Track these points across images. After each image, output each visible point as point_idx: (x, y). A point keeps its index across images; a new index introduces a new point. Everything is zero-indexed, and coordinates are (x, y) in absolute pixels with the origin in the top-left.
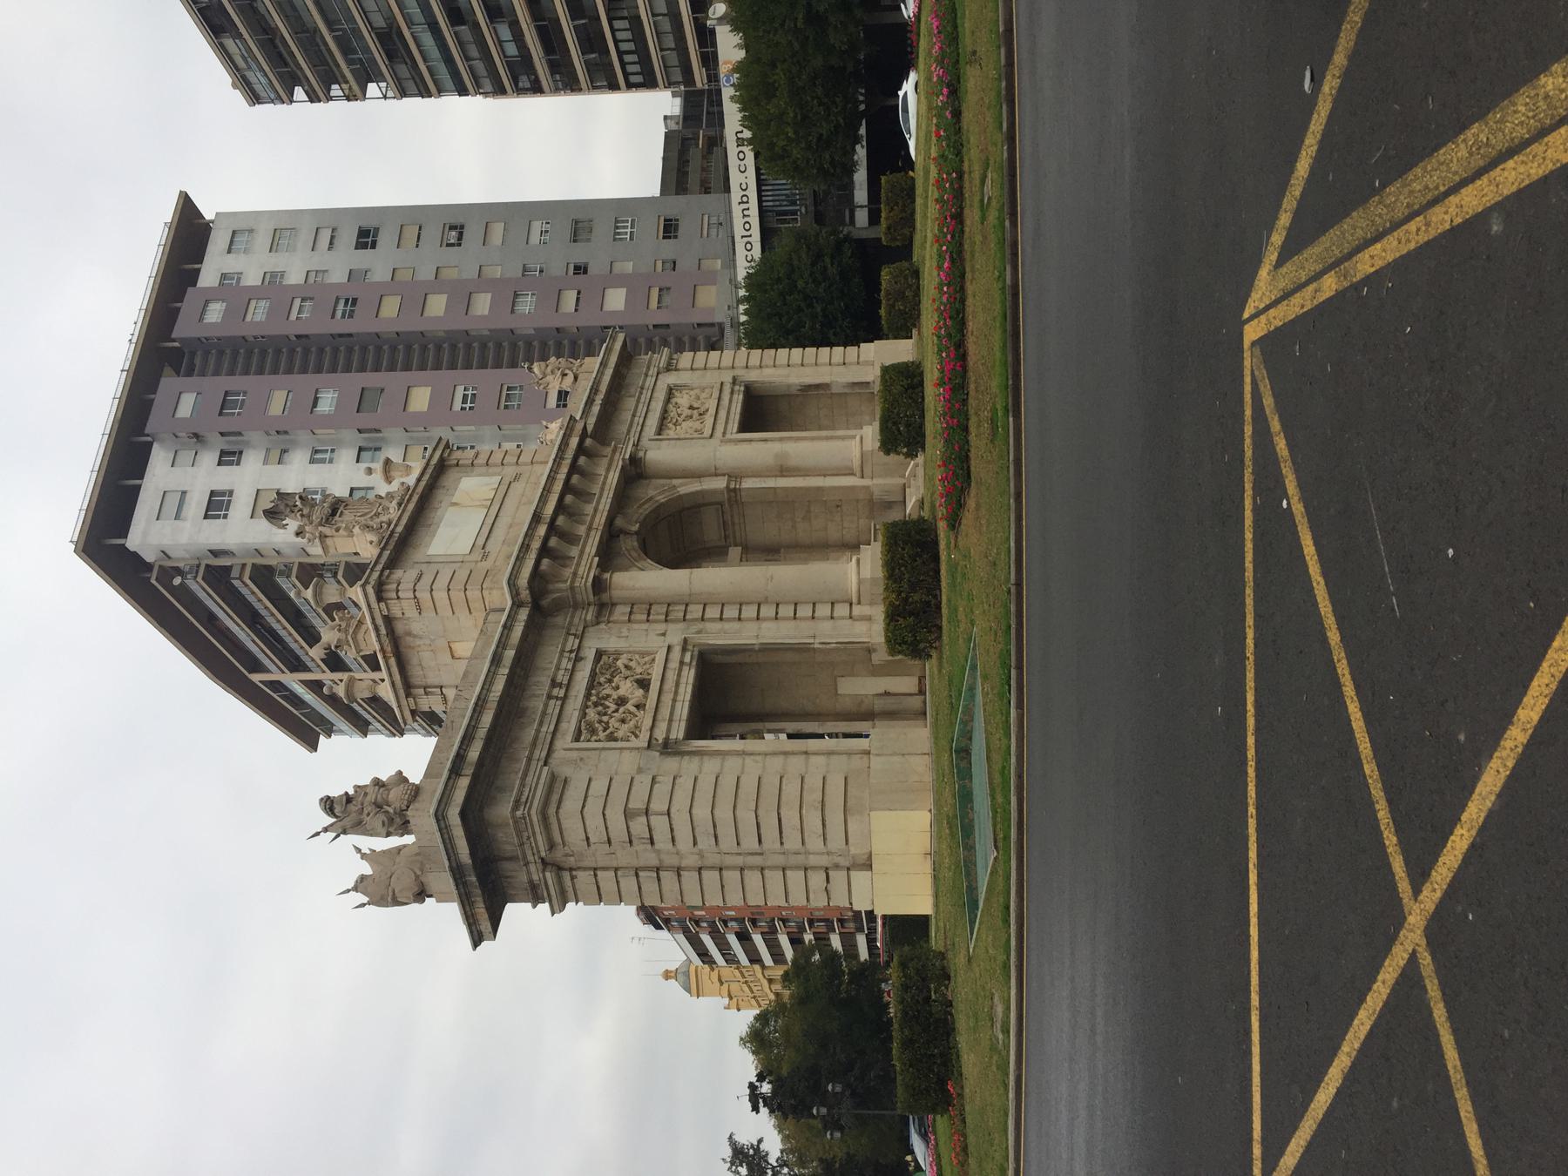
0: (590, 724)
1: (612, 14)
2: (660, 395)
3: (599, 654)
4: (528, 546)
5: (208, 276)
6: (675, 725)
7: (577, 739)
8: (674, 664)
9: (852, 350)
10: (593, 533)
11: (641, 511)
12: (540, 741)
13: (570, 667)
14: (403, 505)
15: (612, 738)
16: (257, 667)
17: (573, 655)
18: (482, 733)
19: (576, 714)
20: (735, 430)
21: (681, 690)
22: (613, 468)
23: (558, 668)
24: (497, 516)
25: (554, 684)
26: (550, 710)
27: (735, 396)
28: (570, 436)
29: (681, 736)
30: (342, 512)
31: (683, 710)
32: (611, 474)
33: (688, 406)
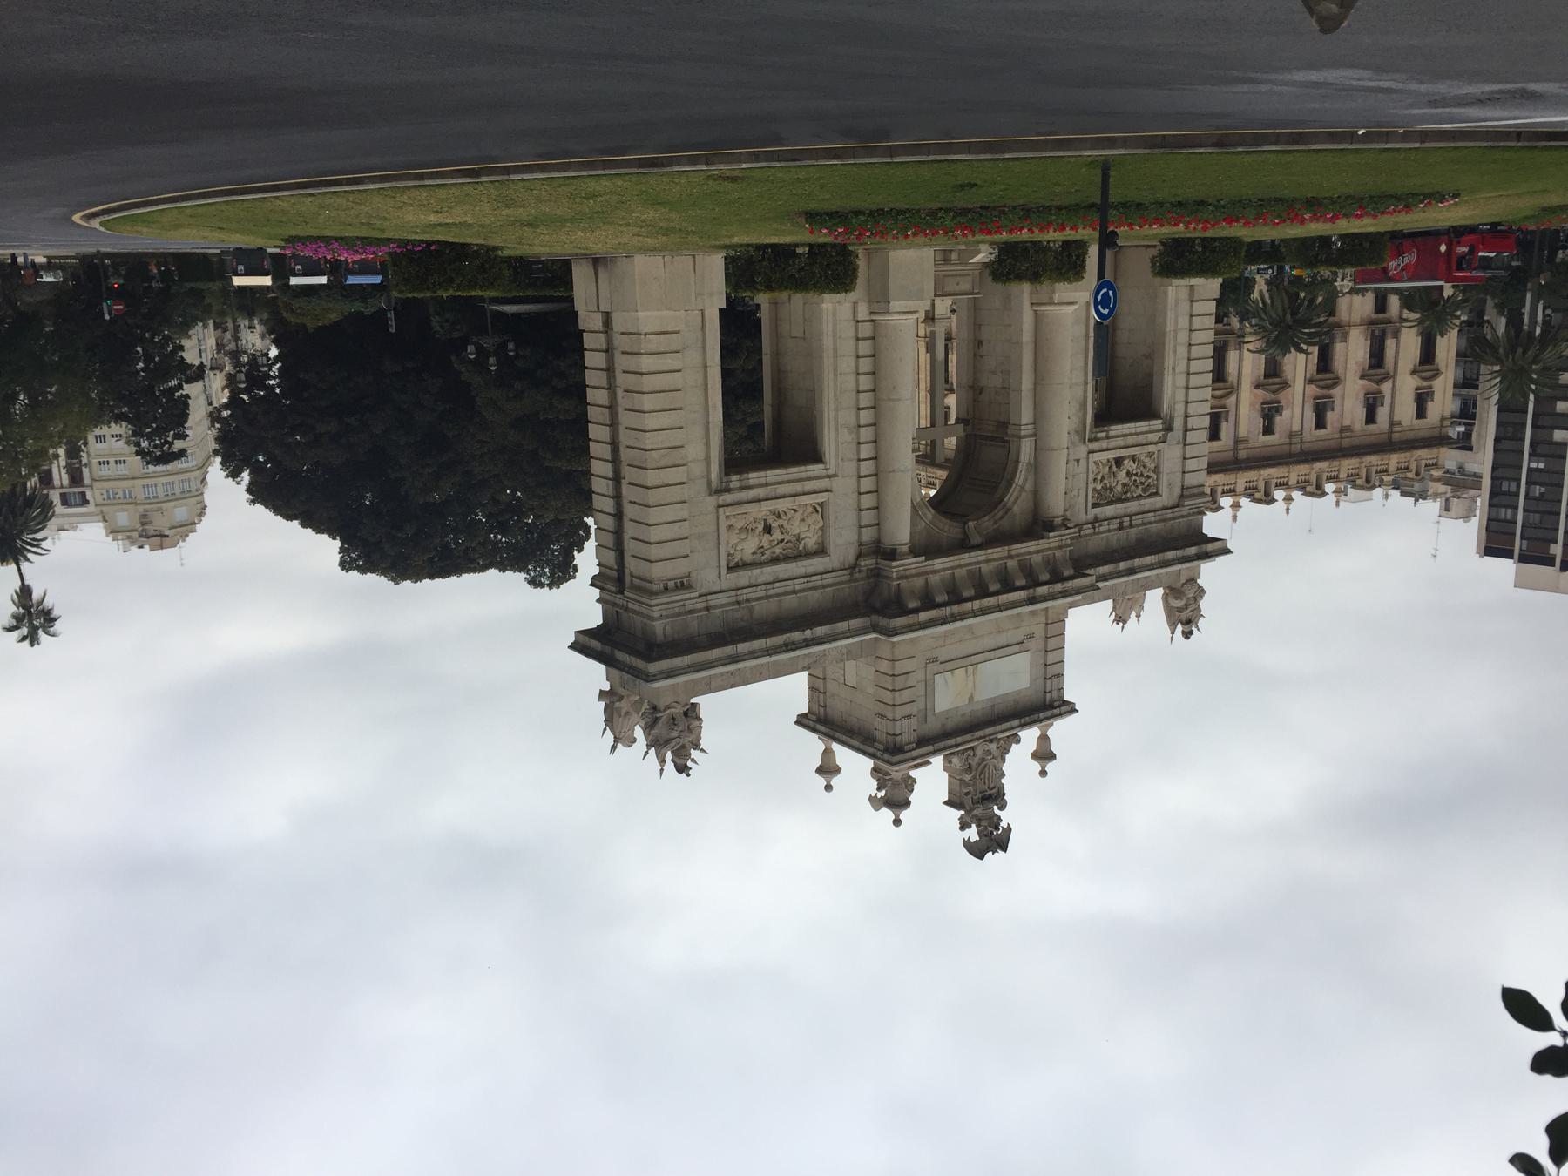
0: (1144, 490)
2: (744, 577)
3: (1094, 505)
4: (1061, 592)
6: (1153, 428)
7: (1157, 494)
8: (1104, 444)
9: (588, 341)
10: (1013, 553)
11: (946, 528)
12: (1161, 517)
13: (1106, 523)
14: (991, 737)
15: (1156, 470)
17: (1097, 525)
18: (1179, 553)
19: (1142, 502)
20: (821, 466)
21: (1127, 432)
22: (929, 568)
23: (1109, 531)
24: (983, 652)
25: (1121, 528)
26: (1140, 521)
27: (752, 482)
28: (919, 624)
29: (1160, 421)
30: (980, 792)
31: (1142, 426)
32: (937, 567)
33: (767, 536)
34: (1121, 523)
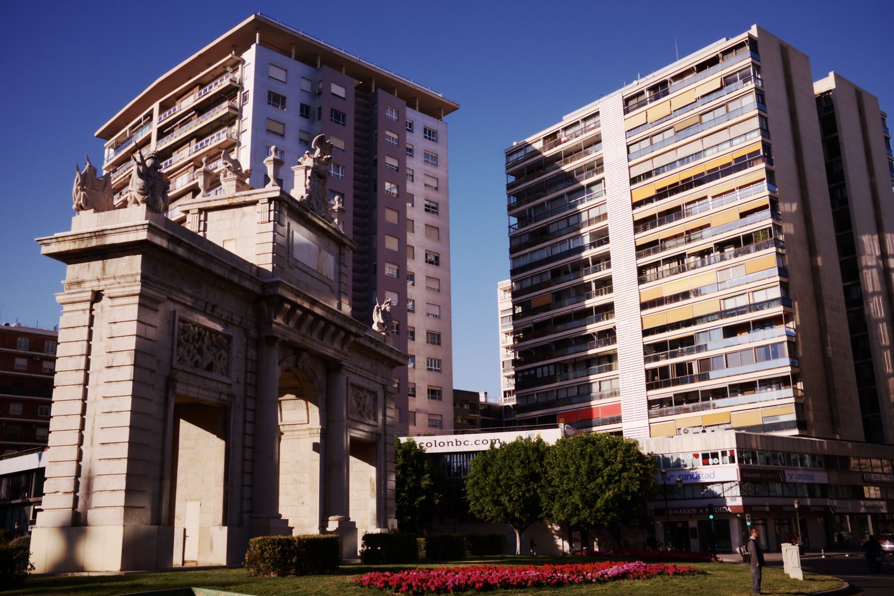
1: (557, 365)
5: (412, 115)
16: (164, 108)
17: (229, 320)
34: (213, 310)
